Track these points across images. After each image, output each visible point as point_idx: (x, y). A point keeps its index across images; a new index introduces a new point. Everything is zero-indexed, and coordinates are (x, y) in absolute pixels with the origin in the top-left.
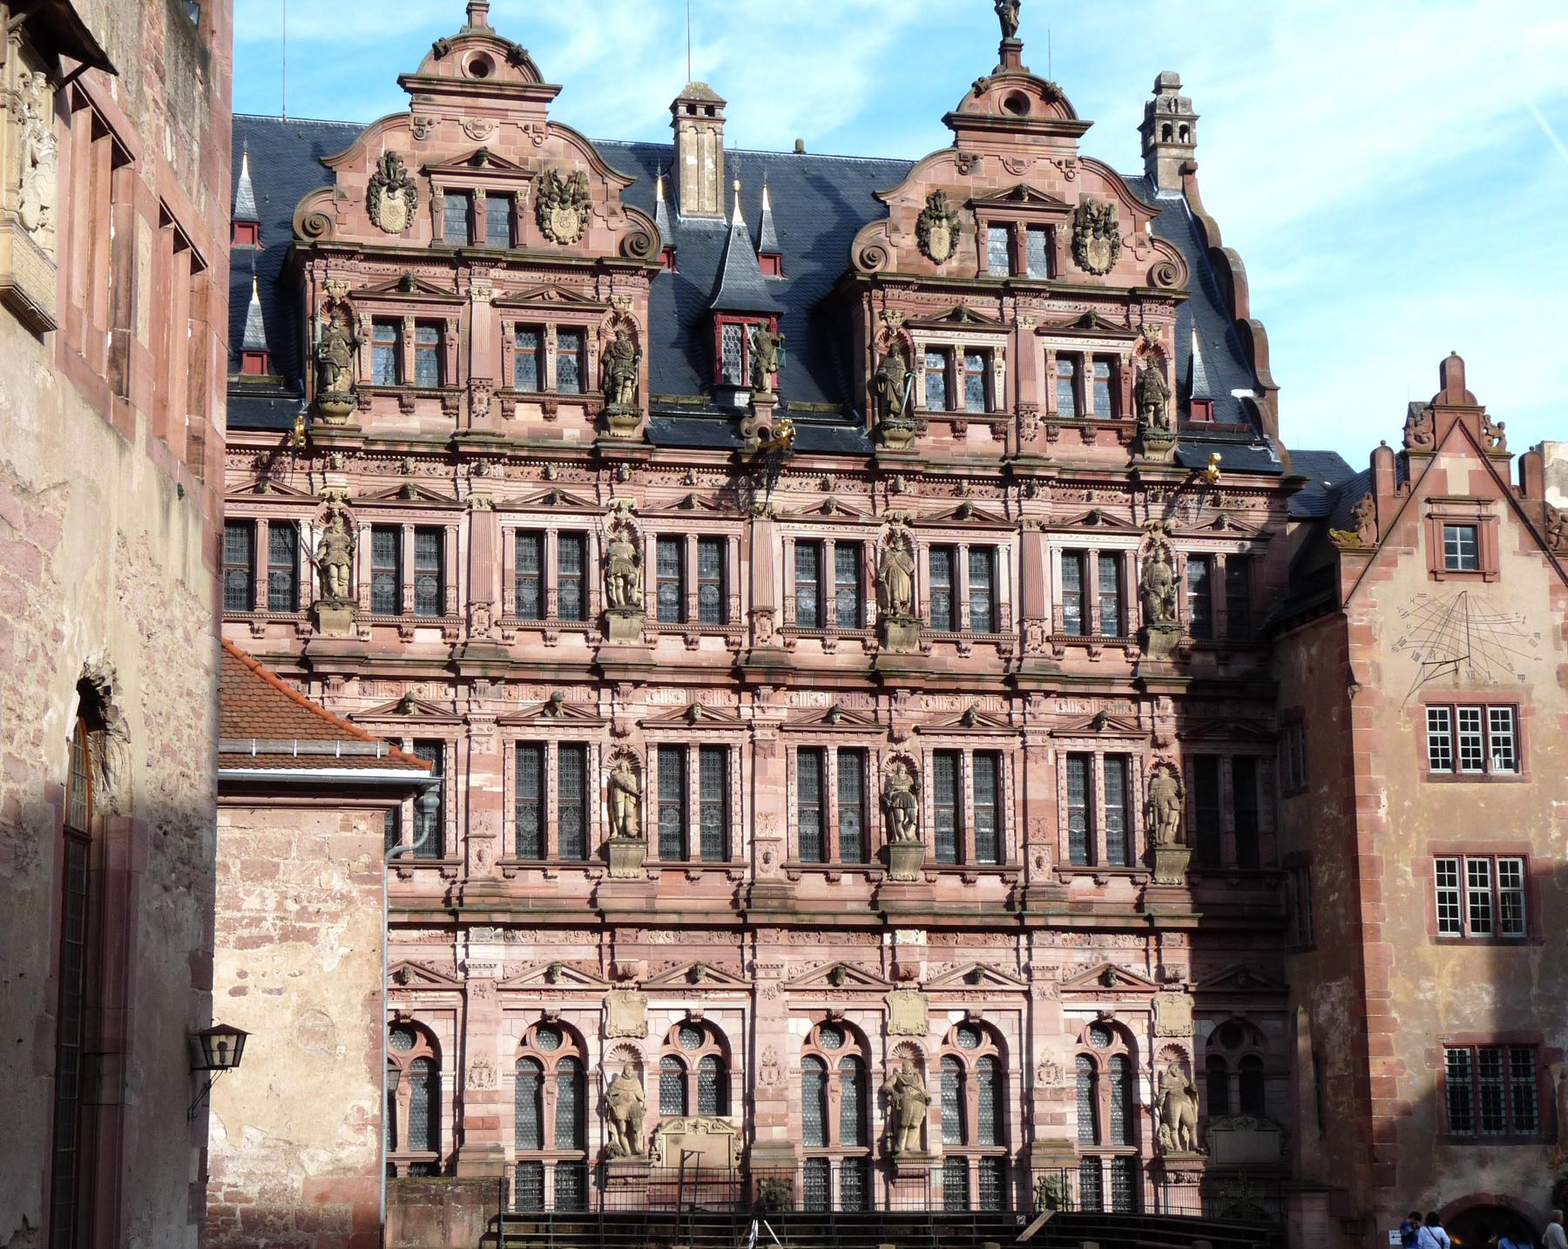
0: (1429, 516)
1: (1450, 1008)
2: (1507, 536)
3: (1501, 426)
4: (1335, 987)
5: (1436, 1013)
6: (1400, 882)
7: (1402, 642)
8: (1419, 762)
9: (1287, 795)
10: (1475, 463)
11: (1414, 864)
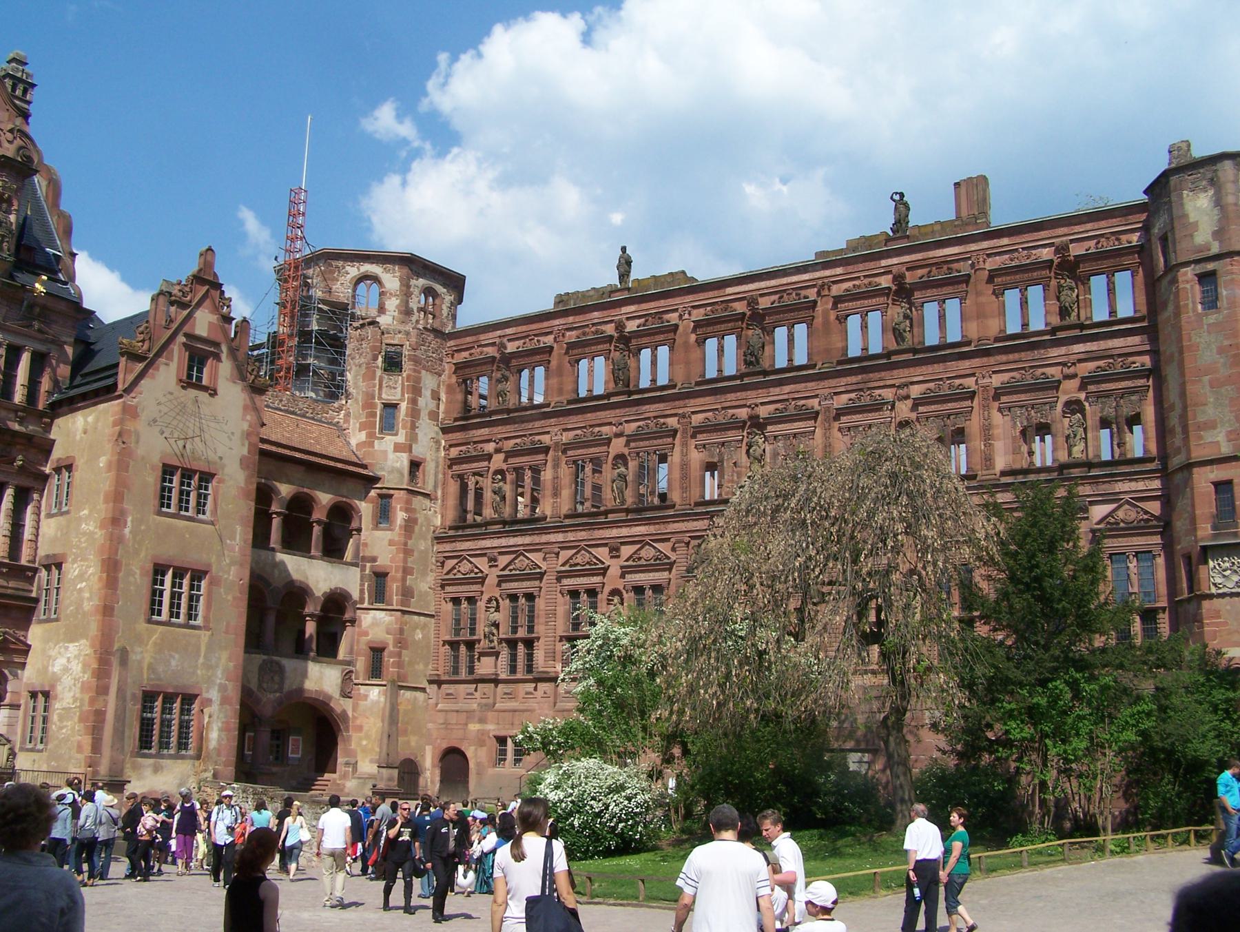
0: (184, 344)
1: (151, 667)
2: (225, 367)
3: (230, 300)
4: (73, 648)
5: (142, 669)
6: (131, 579)
7: (155, 421)
8: (154, 502)
9: (50, 516)
10: (214, 318)
11: (142, 568)
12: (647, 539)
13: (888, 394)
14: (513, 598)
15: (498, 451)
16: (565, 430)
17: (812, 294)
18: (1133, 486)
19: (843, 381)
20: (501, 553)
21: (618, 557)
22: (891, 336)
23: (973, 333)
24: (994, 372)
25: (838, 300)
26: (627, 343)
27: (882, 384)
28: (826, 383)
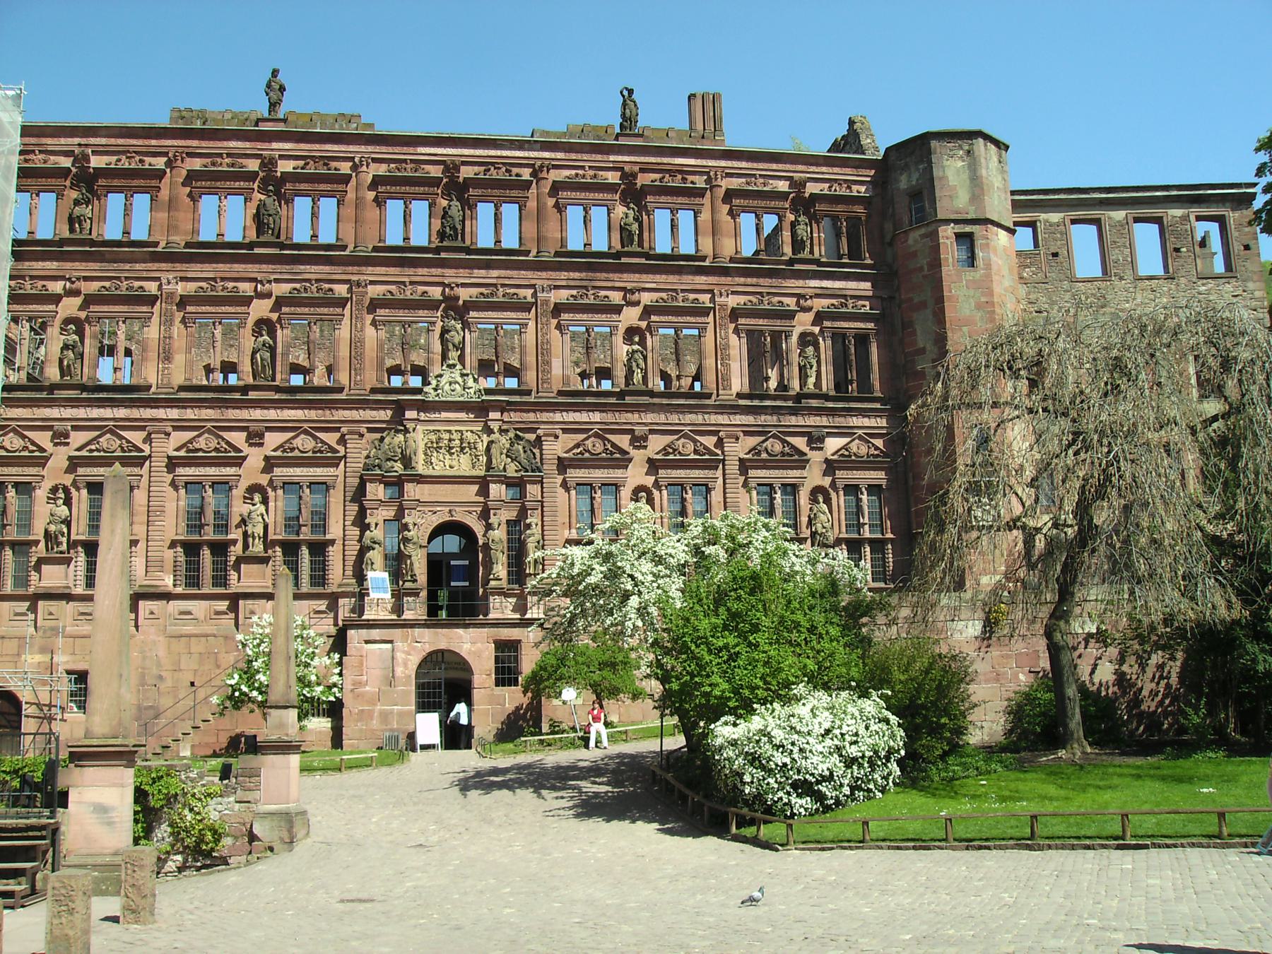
12: (306, 426)
13: (616, 297)
16: (182, 279)
17: (526, 174)
18: (866, 422)
19: (564, 275)
20: (75, 428)
21: (261, 445)
22: (616, 236)
23: (707, 246)
24: (733, 293)
25: (556, 187)
26: (279, 187)
27: (609, 284)
28: (544, 274)
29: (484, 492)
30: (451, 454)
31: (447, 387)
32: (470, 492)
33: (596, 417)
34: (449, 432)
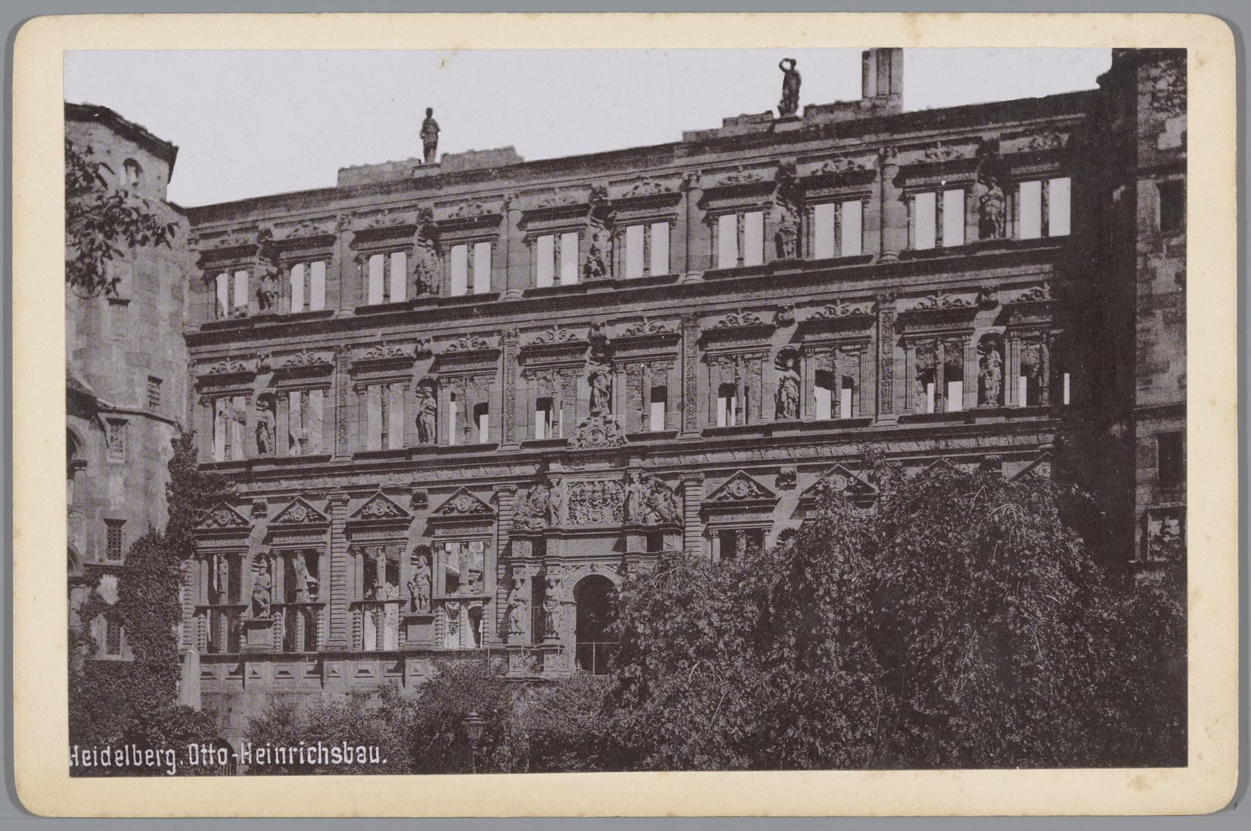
14: (288, 555)
15: (265, 370)
21: (425, 507)
22: (772, 246)
29: (621, 546)
30: (594, 506)
31: (590, 438)
32: (606, 546)
33: (741, 456)
34: (592, 483)
